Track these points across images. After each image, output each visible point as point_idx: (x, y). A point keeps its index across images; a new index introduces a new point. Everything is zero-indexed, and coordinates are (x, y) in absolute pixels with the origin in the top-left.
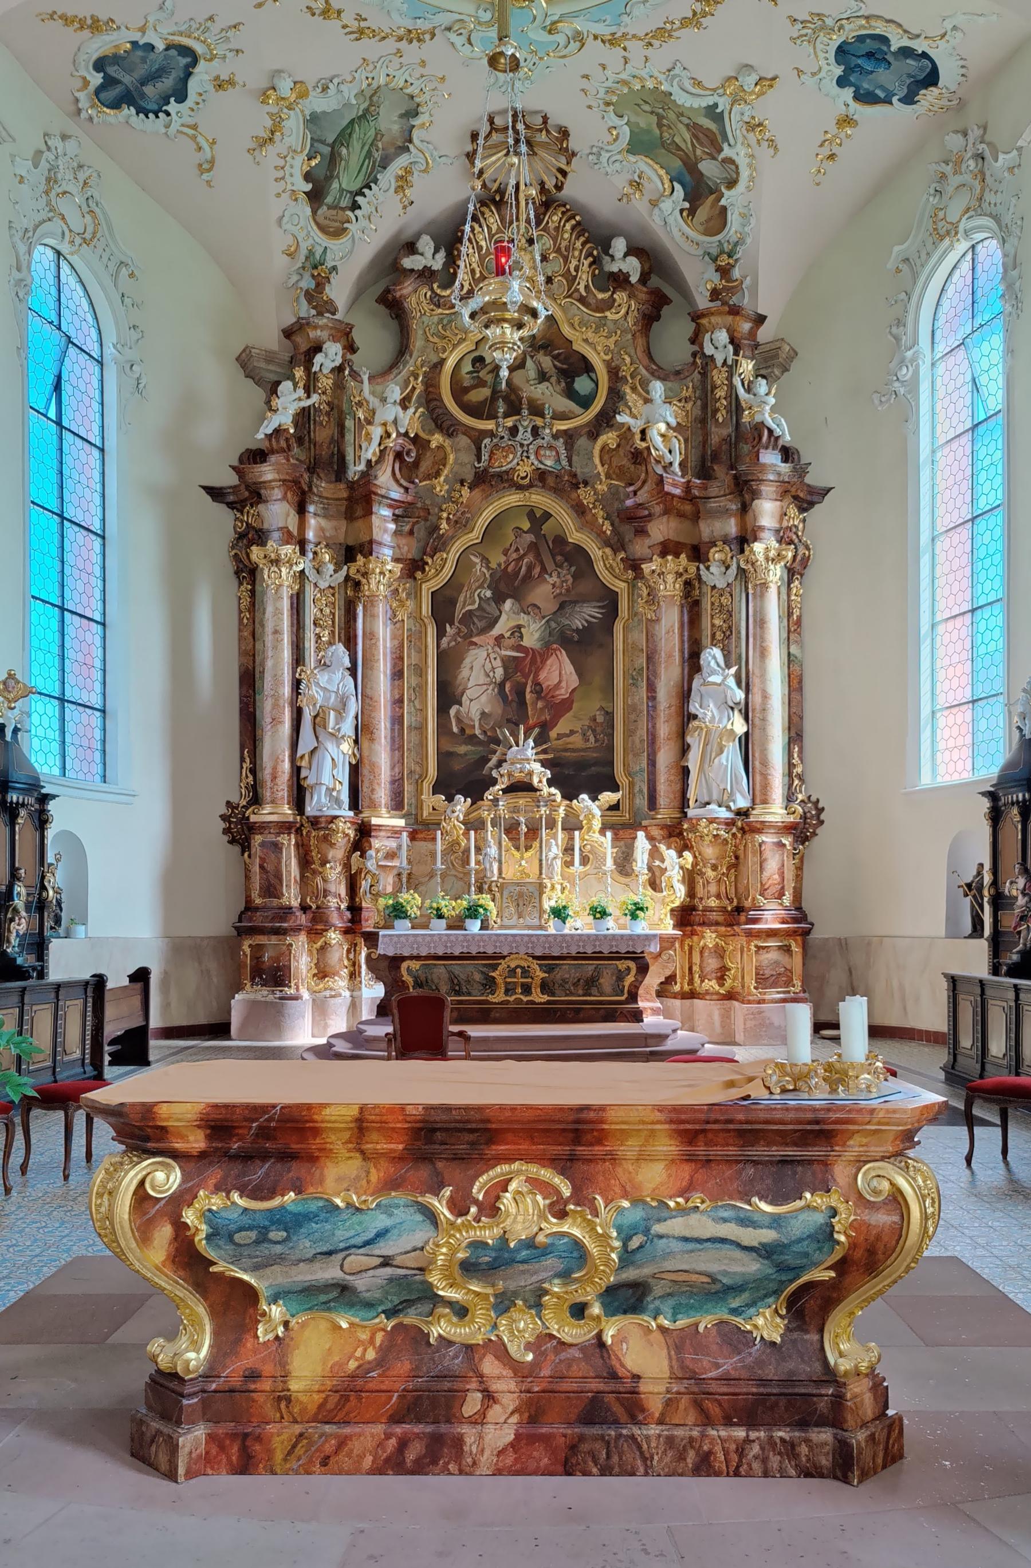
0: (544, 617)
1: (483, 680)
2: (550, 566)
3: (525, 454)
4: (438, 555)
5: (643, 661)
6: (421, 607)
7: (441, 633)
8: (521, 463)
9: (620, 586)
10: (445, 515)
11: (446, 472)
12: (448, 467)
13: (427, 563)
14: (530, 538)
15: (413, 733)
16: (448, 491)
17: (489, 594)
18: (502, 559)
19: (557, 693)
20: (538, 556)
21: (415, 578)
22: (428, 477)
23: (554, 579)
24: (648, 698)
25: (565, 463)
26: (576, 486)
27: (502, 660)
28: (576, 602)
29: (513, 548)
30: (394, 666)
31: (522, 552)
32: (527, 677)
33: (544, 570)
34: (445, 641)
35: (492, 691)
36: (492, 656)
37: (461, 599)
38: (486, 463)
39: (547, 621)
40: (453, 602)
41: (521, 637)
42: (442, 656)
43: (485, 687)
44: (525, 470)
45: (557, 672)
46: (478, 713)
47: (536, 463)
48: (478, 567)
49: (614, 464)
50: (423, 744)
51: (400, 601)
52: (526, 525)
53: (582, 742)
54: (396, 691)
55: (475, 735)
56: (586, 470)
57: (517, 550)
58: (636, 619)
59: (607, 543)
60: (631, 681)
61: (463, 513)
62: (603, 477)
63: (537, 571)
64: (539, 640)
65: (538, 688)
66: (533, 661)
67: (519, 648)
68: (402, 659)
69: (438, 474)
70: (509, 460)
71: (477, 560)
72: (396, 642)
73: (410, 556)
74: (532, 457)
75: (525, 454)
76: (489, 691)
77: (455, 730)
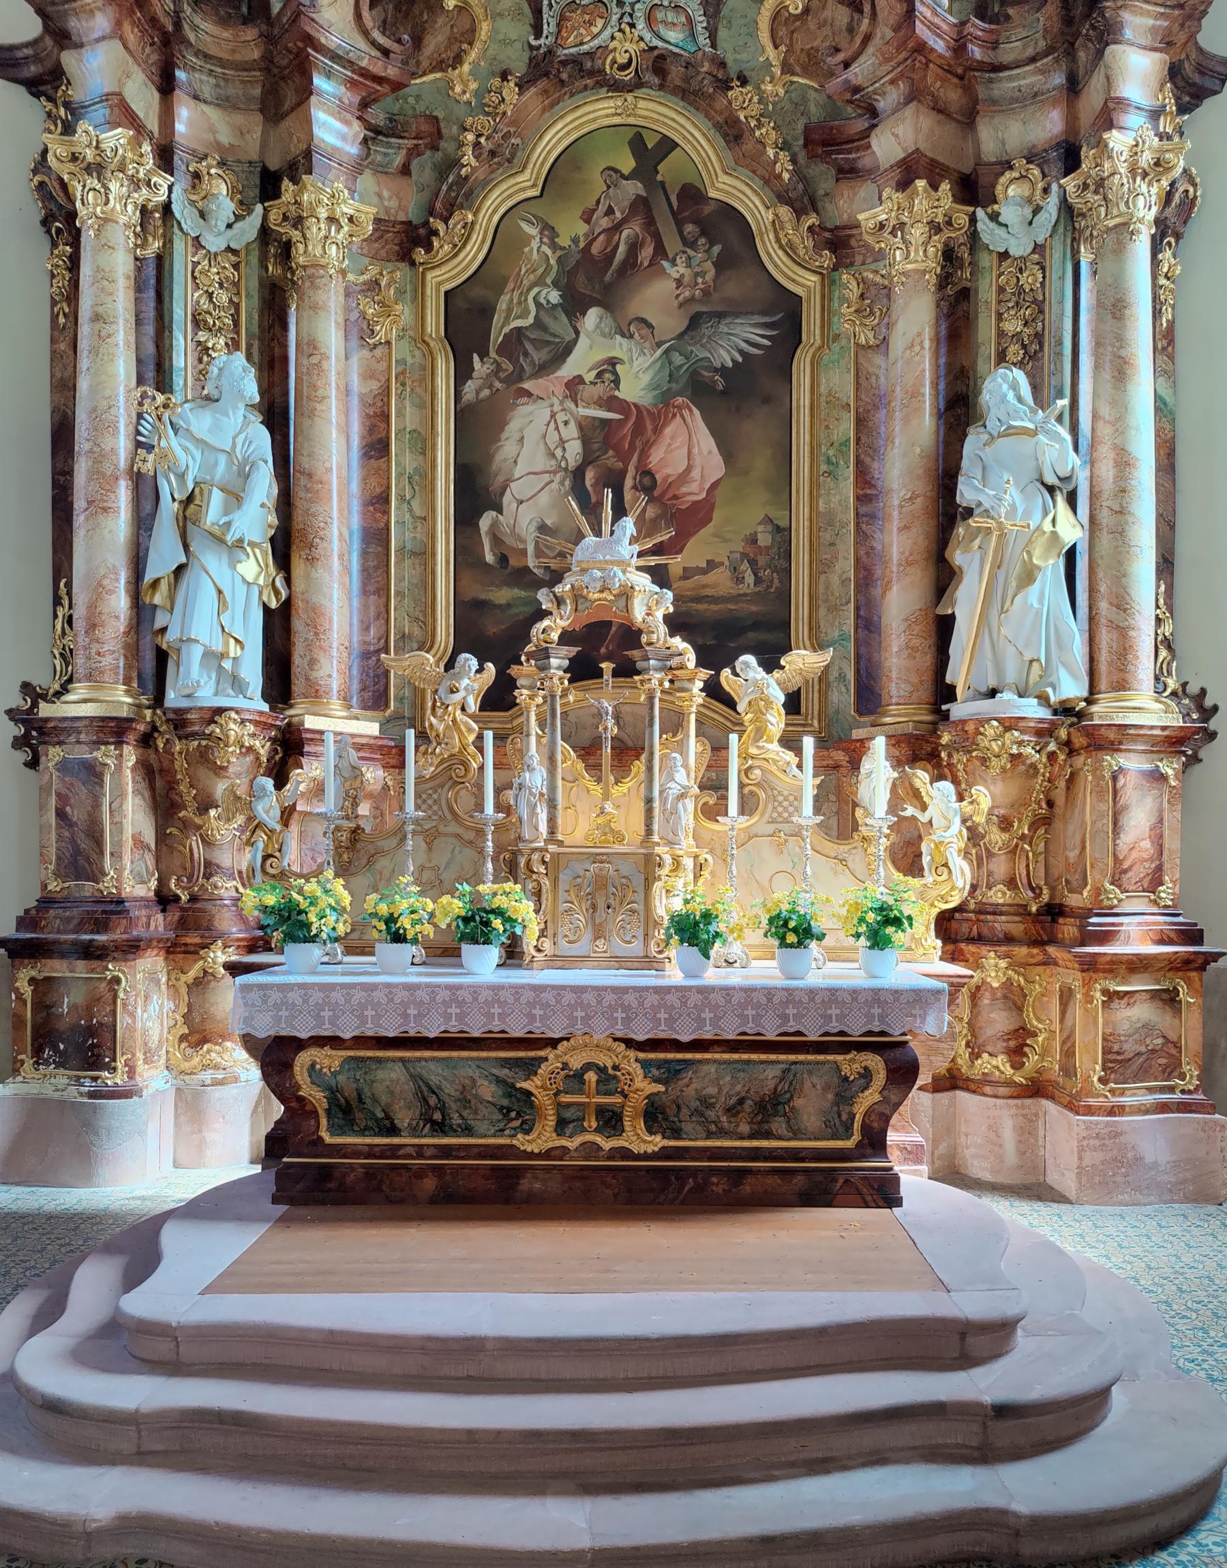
0: (659, 345)
1: (542, 463)
2: (672, 243)
3: (627, 19)
4: (457, 216)
5: (846, 427)
6: (423, 318)
7: (463, 373)
8: (618, 35)
9: (804, 283)
10: (470, 137)
11: (473, 55)
12: (478, 46)
13: (435, 233)
14: (634, 188)
15: (407, 562)
16: (476, 93)
17: (554, 297)
18: (582, 229)
19: (684, 490)
20: (650, 224)
21: (413, 263)
22: (440, 66)
23: (680, 269)
24: (858, 498)
25: (703, 40)
26: (725, 85)
27: (581, 428)
28: (720, 316)
29: (602, 208)
30: (371, 429)
31: (618, 215)
32: (626, 459)
33: (660, 251)
34: (470, 387)
35: (560, 484)
36: (561, 417)
37: (502, 305)
38: (551, 40)
39: (666, 352)
40: (485, 312)
41: (616, 382)
42: (465, 417)
43: (547, 477)
44: (625, 49)
45: (685, 450)
46: (532, 528)
47: (648, 36)
48: (535, 244)
49: (798, 47)
50: (426, 584)
51: (382, 303)
52: (627, 163)
53: (729, 583)
54: (373, 482)
55: (526, 569)
56: (744, 56)
57: (610, 211)
58: (836, 347)
59: (783, 198)
60: (824, 467)
61: (507, 136)
62: (777, 71)
63: (647, 253)
64: (653, 386)
65: (647, 481)
66: (638, 429)
67: (612, 403)
68: (386, 417)
69: (458, 60)
70: (595, 30)
71: (532, 231)
72: (375, 385)
73: (402, 217)
74: (641, 25)
75: (627, 19)
76: (554, 486)
77: (489, 558)
